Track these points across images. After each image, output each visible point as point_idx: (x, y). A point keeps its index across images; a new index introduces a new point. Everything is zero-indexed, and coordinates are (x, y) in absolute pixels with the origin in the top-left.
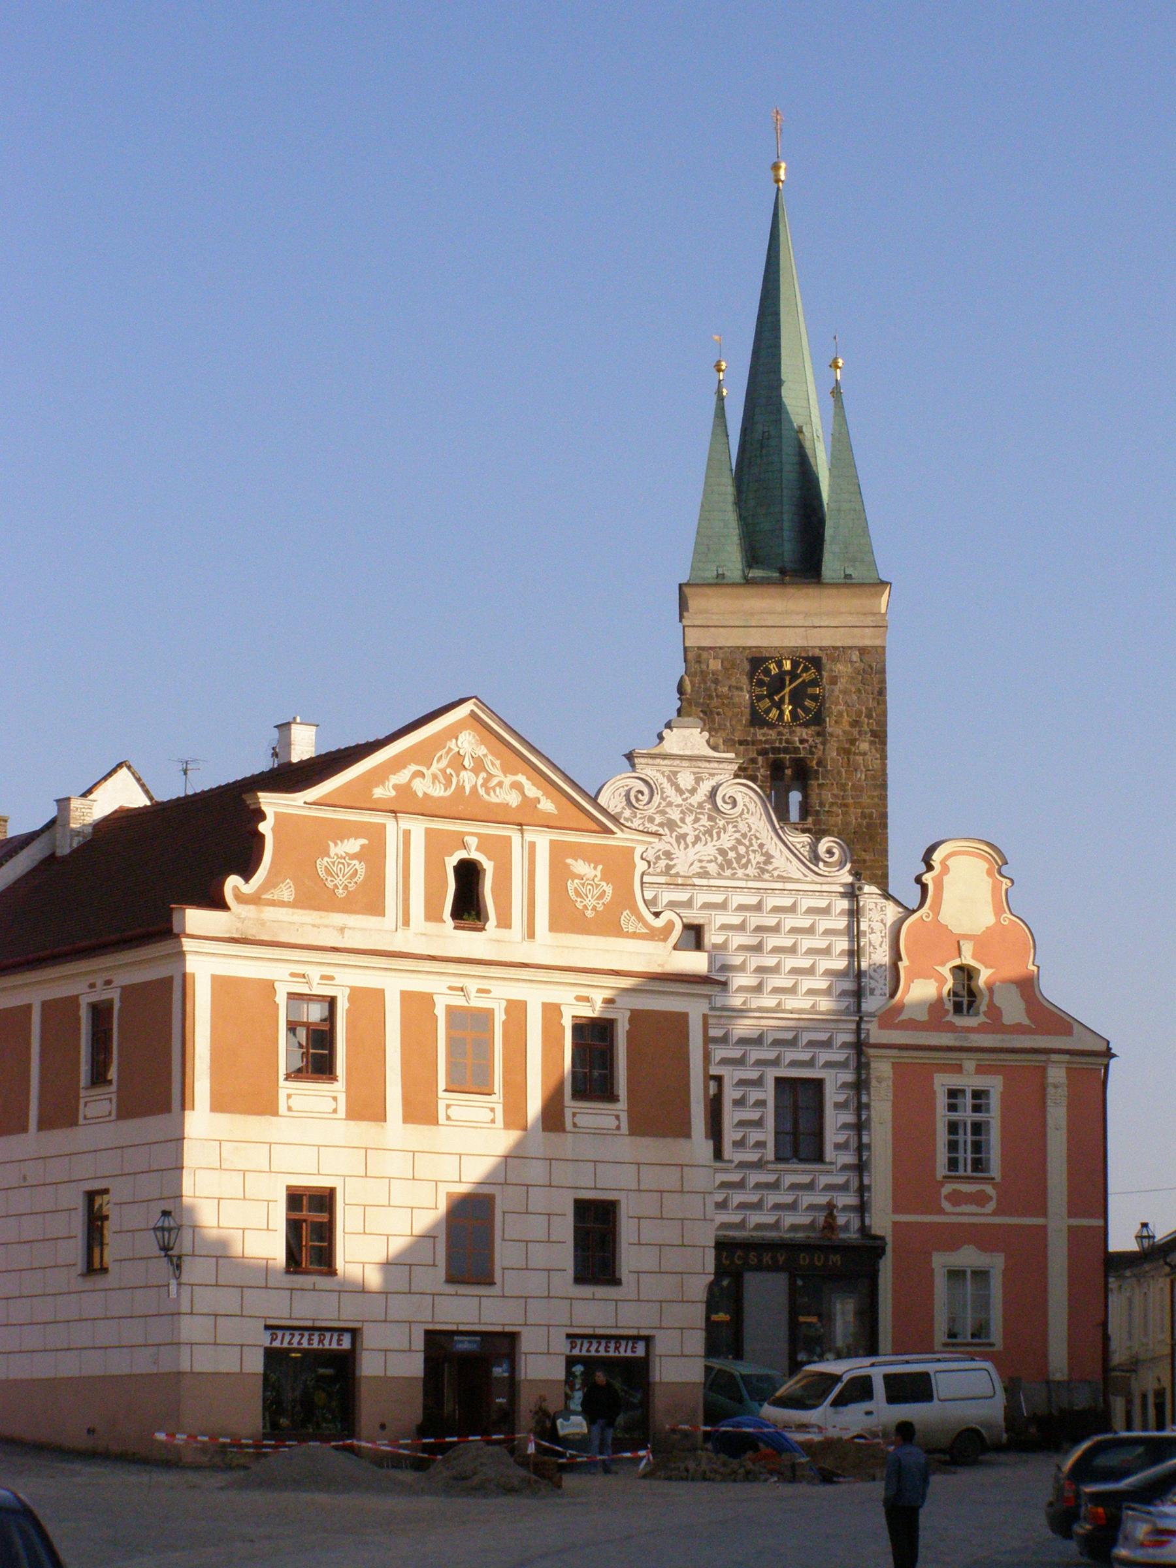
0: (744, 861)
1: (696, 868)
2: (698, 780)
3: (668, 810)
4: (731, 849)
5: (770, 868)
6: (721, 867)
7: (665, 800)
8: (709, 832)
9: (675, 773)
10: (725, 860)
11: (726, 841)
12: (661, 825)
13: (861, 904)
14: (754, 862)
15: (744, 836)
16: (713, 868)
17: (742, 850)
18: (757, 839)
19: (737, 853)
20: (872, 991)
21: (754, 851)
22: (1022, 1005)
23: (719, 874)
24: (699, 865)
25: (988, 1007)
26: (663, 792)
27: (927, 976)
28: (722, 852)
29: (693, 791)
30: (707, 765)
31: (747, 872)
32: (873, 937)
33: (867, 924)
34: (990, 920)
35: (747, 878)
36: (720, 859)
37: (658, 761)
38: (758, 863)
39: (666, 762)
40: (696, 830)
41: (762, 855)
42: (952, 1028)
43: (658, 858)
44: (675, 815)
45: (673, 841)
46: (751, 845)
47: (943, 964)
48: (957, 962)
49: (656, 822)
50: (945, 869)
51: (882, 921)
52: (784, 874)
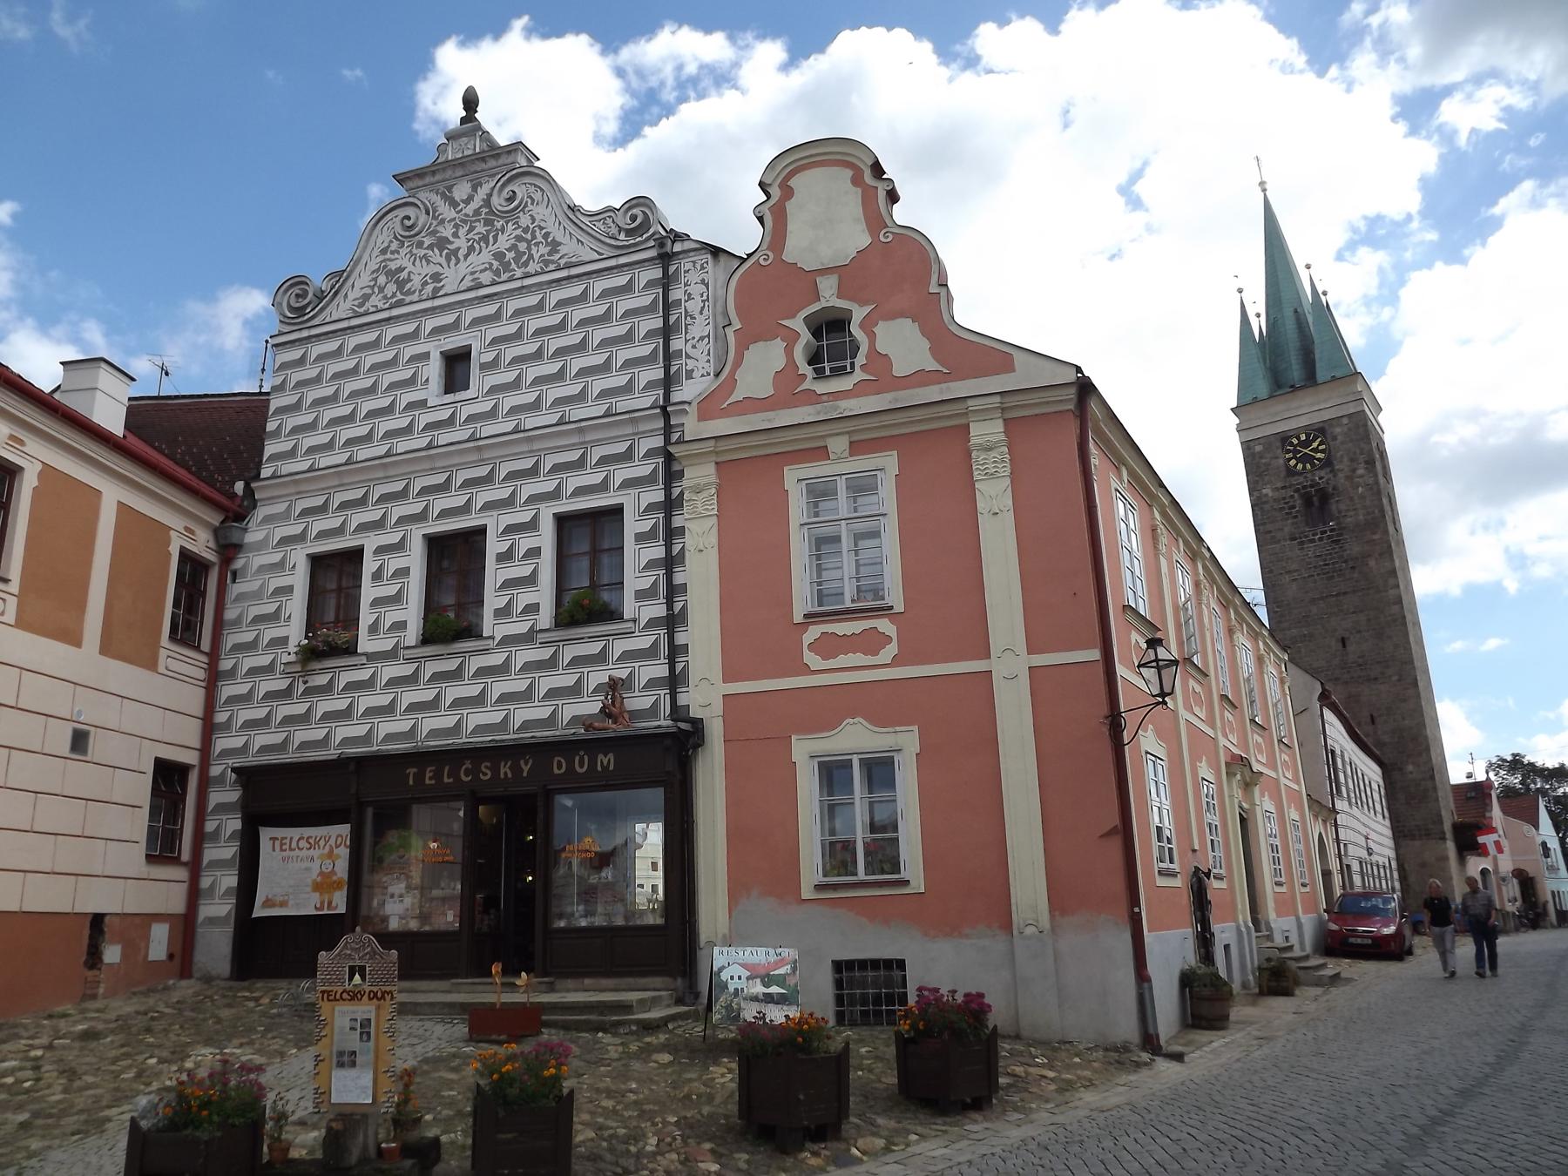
1: (467, 283)
2: (475, 189)
3: (440, 228)
4: (509, 250)
5: (557, 256)
7: (434, 218)
8: (485, 239)
9: (450, 189)
11: (504, 242)
12: (431, 247)
14: (536, 257)
15: (526, 230)
16: (486, 278)
18: (541, 228)
20: (690, 375)
28: (499, 256)
30: (484, 166)
36: (496, 264)
37: (428, 180)
39: (438, 177)
42: (812, 398)
43: (425, 283)
44: (447, 232)
45: (443, 261)
46: (534, 237)
47: (793, 316)
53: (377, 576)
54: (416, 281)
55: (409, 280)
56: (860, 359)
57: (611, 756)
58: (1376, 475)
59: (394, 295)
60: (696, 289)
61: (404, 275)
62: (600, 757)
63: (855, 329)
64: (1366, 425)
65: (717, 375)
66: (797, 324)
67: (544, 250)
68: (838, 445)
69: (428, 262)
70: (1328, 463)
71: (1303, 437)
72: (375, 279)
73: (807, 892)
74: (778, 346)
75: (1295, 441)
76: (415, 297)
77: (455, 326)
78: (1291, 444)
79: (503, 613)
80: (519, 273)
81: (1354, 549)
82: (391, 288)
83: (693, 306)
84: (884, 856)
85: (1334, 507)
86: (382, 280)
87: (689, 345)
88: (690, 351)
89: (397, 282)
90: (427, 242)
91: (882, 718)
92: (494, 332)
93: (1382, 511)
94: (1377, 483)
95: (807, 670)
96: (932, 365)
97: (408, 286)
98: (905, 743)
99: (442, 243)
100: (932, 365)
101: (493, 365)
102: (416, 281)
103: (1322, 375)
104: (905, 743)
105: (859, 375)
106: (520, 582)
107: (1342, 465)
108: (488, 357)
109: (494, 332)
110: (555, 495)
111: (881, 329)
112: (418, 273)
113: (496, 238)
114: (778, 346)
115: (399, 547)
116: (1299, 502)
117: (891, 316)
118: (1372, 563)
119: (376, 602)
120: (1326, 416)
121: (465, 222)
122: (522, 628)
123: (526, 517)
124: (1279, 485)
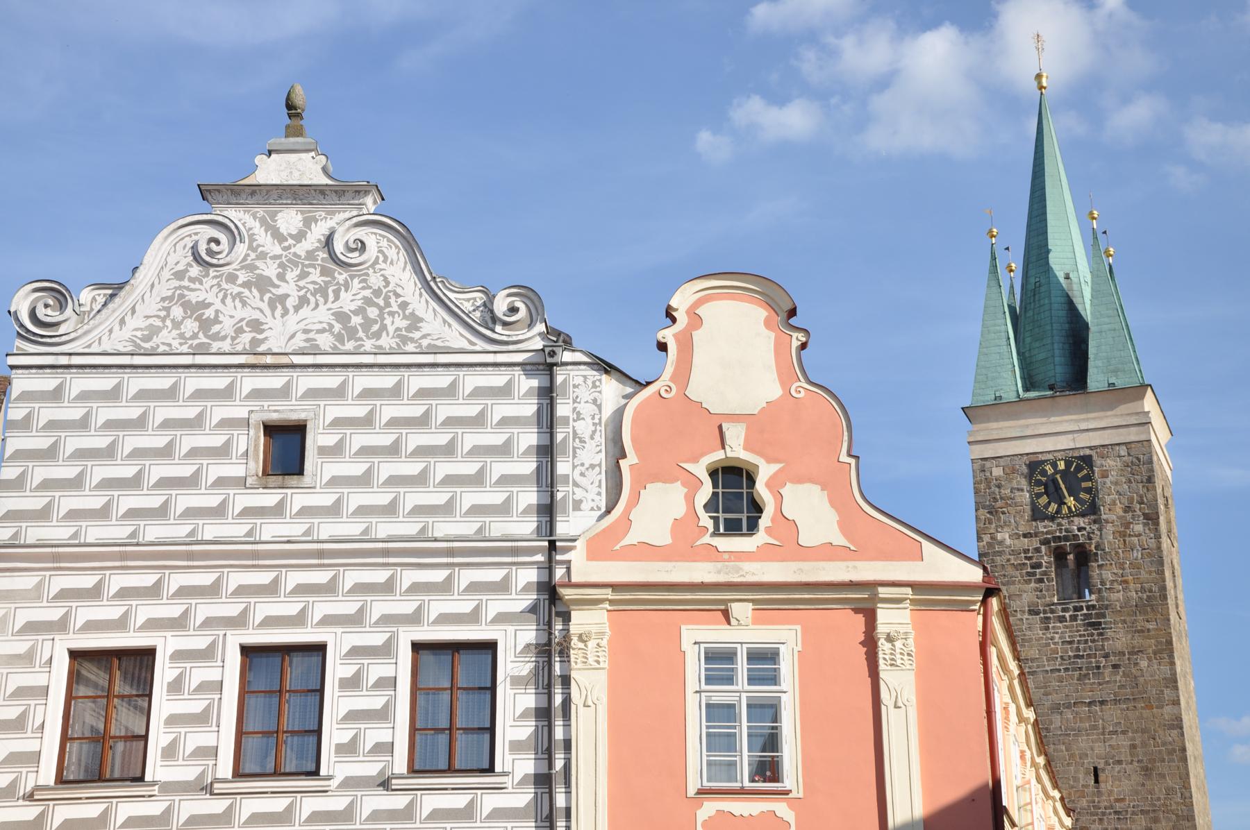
0: (376, 328)
1: (299, 342)
2: (308, 222)
3: (259, 263)
4: (356, 313)
5: (416, 335)
6: (339, 338)
7: (254, 250)
8: (323, 291)
9: (273, 216)
11: (348, 302)
12: (247, 285)
14: (391, 329)
15: (377, 293)
16: (325, 341)
17: (373, 312)
18: (397, 295)
19: (366, 318)
20: (577, 505)
21: (392, 314)
22: (832, 517)
23: (335, 347)
24: (304, 336)
25: (773, 520)
26: (252, 239)
28: (342, 317)
29: (300, 236)
31: (379, 343)
32: (580, 426)
33: (571, 407)
34: (776, 392)
35: (380, 351)
36: (337, 327)
38: (398, 329)
40: (301, 288)
41: (405, 317)
42: (713, 554)
43: (239, 331)
44: (270, 270)
45: (265, 306)
46: (388, 305)
47: (695, 460)
48: (718, 455)
49: (240, 281)
50: (696, 320)
51: (595, 401)
52: (439, 343)
53: (176, 686)
54: (227, 326)
55: (216, 321)
56: (765, 521)
58: (1158, 537)
59: (195, 336)
60: (587, 409)
61: (209, 313)
63: (761, 488)
64: (1150, 462)
65: (608, 512)
66: (700, 470)
67: (401, 323)
68: (742, 611)
69: (244, 304)
70: (1092, 509)
71: (1062, 465)
72: (168, 309)
75: (1049, 469)
77: (284, 392)
78: (1044, 473)
79: (348, 749)
80: (368, 345)
81: (1118, 638)
82: (190, 326)
83: (584, 428)
85: (1095, 573)
86: (177, 312)
87: (577, 471)
88: (579, 479)
90: (243, 277)
92: (335, 410)
93: (1163, 588)
94: (1159, 548)
96: (839, 540)
99: (262, 284)
100: (839, 540)
101: (335, 451)
102: (227, 326)
103: (1096, 379)
105: (761, 538)
107: (1112, 513)
108: (330, 440)
109: (335, 410)
110: (414, 619)
111: (788, 491)
112: (231, 315)
115: (206, 655)
116: (1046, 559)
117: (799, 480)
118: (1144, 664)
119: (173, 720)
120: (1096, 439)
122: (372, 769)
123: (377, 639)
124: (1021, 531)
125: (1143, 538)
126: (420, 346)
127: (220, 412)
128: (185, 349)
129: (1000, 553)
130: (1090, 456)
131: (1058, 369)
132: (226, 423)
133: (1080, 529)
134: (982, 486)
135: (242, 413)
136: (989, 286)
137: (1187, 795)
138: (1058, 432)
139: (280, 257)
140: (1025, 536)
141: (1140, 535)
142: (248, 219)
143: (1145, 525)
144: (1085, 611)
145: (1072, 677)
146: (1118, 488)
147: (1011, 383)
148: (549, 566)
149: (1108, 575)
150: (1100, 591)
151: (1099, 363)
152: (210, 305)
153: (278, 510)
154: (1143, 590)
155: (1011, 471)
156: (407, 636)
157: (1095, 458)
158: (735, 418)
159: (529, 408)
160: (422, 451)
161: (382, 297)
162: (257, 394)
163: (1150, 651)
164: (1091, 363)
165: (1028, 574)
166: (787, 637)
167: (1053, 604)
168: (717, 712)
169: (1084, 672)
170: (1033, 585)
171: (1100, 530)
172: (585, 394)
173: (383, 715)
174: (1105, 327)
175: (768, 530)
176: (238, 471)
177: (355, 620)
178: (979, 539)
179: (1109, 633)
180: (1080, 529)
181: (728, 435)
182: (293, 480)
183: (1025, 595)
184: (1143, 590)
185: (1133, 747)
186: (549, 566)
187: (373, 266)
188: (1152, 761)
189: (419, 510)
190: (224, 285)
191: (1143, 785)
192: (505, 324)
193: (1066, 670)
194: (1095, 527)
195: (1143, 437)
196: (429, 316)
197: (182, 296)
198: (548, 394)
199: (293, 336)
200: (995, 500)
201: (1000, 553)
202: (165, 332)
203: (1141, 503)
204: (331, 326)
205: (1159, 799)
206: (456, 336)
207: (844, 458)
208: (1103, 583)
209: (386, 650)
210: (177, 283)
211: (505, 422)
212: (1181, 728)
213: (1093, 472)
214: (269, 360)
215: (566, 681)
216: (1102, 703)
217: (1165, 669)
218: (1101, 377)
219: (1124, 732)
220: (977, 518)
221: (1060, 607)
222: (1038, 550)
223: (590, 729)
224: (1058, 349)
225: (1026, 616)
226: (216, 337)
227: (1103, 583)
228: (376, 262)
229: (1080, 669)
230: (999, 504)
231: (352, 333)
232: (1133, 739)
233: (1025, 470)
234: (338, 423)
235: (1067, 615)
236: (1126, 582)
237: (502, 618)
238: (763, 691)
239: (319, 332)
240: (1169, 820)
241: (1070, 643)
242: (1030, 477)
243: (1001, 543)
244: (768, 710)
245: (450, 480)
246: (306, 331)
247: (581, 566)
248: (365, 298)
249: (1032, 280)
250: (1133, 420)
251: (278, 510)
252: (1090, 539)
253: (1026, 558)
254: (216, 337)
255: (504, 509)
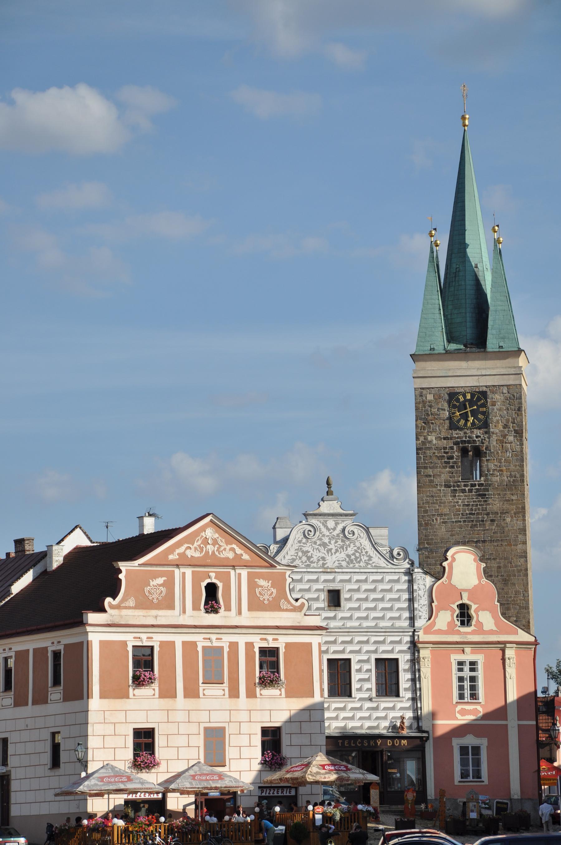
0: (359, 560)
1: (336, 564)
2: (337, 524)
3: (323, 538)
4: (353, 555)
5: (371, 562)
6: (348, 563)
9: (326, 521)
10: (350, 560)
11: (350, 551)
13: (414, 577)
14: (363, 560)
15: (358, 548)
16: (344, 564)
17: (358, 555)
18: (365, 549)
19: (355, 556)
20: (420, 617)
21: (363, 555)
23: (347, 566)
26: (320, 530)
27: (446, 610)
28: (348, 556)
29: (334, 529)
32: (420, 592)
34: (476, 582)
35: (360, 567)
36: (347, 559)
41: (367, 556)
42: (459, 633)
43: (319, 560)
44: (326, 540)
45: (325, 552)
46: (362, 552)
48: (460, 602)
50: (454, 559)
51: (424, 584)
52: (378, 565)
55: (312, 557)
56: (474, 622)
57: (406, 741)
59: (306, 562)
60: (422, 587)
61: (309, 554)
62: (402, 741)
64: (521, 398)
65: (429, 619)
68: (468, 650)
69: (319, 551)
70: (485, 425)
71: (469, 397)
72: (297, 553)
73: (456, 783)
74: (449, 613)
75: (461, 399)
76: (315, 565)
77: (333, 580)
78: (458, 400)
79: (359, 690)
81: (495, 504)
82: (304, 559)
83: (421, 593)
84: (477, 775)
86: (300, 554)
87: (420, 606)
88: (420, 609)
89: (306, 556)
90: (318, 542)
91: (477, 735)
92: (348, 586)
93: (522, 476)
95: (457, 719)
96: (495, 629)
97: (312, 559)
98: (483, 743)
99: (324, 545)
100: (495, 629)
101: (349, 599)
102: (315, 559)
103: (492, 343)
104: (483, 743)
106: (363, 678)
107: (496, 428)
108: (347, 596)
109: (348, 586)
110: (375, 651)
111: (480, 613)
112: (316, 555)
113: (346, 548)
114: (449, 613)
117: (483, 610)
118: (508, 520)
120: (490, 381)
121: (334, 538)
122: (366, 695)
125: (513, 444)
126: (372, 566)
127: (316, 586)
128: (303, 566)
129: (429, 448)
130: (486, 392)
131: (468, 331)
132: (317, 590)
133: (477, 437)
134: (420, 406)
135: (321, 587)
136: (428, 271)
137: (526, 595)
138: (468, 374)
139: (329, 536)
140: (445, 439)
141: (511, 443)
142: (318, 523)
143: (515, 436)
144: (477, 487)
145: (467, 526)
146: (501, 413)
147: (439, 341)
148: (413, 636)
149: (492, 466)
150: (486, 475)
151: (494, 332)
152: (309, 552)
153: (334, 618)
154: (511, 476)
155: (438, 397)
156: (374, 657)
157: (489, 393)
158: (465, 590)
159: (405, 586)
160: (375, 600)
161: (359, 549)
162: (325, 581)
163: (513, 512)
164: (489, 332)
165: (445, 462)
166: (480, 658)
167: (459, 482)
168: (461, 679)
169: (474, 523)
170: (448, 469)
171: (489, 438)
172: (421, 582)
173: (368, 680)
174: (499, 308)
175: (474, 625)
176: (322, 605)
177: (359, 652)
178: (417, 439)
179: (490, 501)
180: (477, 437)
181: (463, 596)
182: (338, 608)
183: (443, 475)
184: (511, 476)
185: (499, 567)
186: (413, 636)
187: (356, 539)
188: (509, 576)
189: (375, 618)
190: (313, 545)
191: (503, 589)
192: (397, 559)
193: (464, 521)
194: (486, 436)
195: (517, 382)
196: (374, 556)
197: (301, 549)
198: (411, 582)
199: (334, 562)
200: (428, 415)
201: (429, 448)
202: (297, 560)
203: (513, 423)
204: (346, 559)
205: (511, 597)
206: (382, 562)
207: (496, 603)
208: (488, 471)
209: (368, 661)
210: (299, 545)
211: (398, 591)
212: (526, 557)
213: (487, 402)
214: (329, 570)
215: (419, 670)
216: (484, 541)
217: (520, 523)
218: (495, 341)
219: (494, 559)
220: (417, 426)
221: (463, 484)
222: (452, 448)
223: (426, 684)
224: (468, 315)
225: (443, 488)
226: (312, 562)
227: (488, 471)
228: (357, 538)
229: (472, 521)
230: (430, 417)
231: (352, 561)
232: (499, 563)
233: (447, 397)
234: (350, 590)
235: (467, 489)
236: (502, 471)
237: (400, 652)
238: (473, 674)
239: (342, 561)
240: (515, 609)
241: (468, 505)
242: (449, 402)
243: (430, 442)
244: (473, 679)
245: (383, 609)
246: (338, 561)
247: (422, 636)
248: (355, 550)
249: (454, 266)
250: (512, 371)
251: (334, 618)
252: (483, 443)
253: (445, 453)
254: (312, 562)
255: (399, 618)
